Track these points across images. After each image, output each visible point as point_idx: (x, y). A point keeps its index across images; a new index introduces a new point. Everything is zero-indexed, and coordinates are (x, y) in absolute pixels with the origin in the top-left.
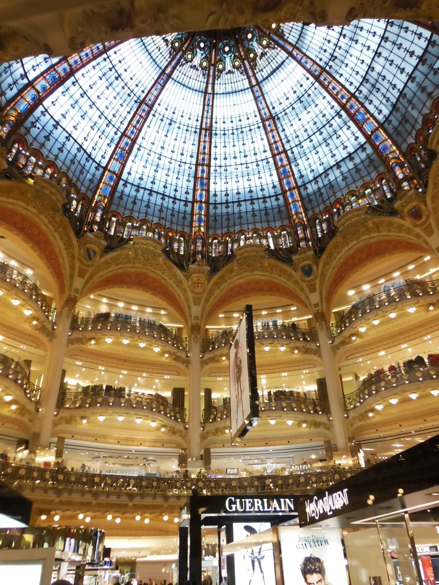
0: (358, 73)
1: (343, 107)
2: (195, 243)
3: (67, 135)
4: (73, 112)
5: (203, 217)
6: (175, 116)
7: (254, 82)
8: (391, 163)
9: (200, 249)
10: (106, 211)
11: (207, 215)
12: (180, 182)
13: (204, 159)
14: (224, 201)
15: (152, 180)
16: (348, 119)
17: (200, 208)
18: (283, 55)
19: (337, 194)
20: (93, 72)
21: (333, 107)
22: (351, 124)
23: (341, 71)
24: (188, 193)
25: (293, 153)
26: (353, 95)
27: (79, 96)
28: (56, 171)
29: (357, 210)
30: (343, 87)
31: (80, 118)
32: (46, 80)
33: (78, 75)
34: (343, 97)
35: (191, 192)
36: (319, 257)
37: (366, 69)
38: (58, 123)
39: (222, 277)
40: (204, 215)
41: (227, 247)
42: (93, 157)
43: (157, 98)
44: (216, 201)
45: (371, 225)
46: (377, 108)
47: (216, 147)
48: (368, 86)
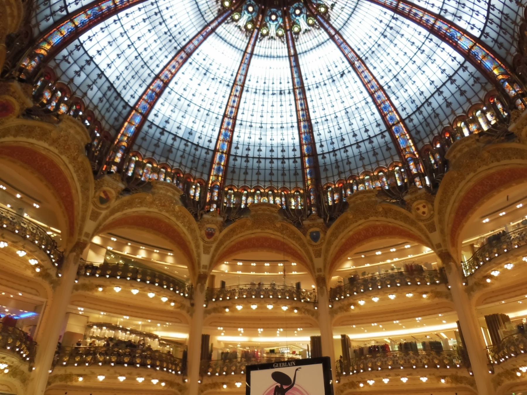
1: (371, 95)
2: (212, 192)
3: (100, 73)
4: (109, 49)
5: (222, 167)
8: (406, 157)
9: (216, 198)
10: (127, 151)
11: (226, 165)
12: (205, 130)
13: (231, 112)
14: (244, 155)
17: (221, 158)
18: (326, 36)
20: (138, 13)
27: (119, 34)
28: (83, 109)
29: (370, 191)
30: (374, 78)
31: (116, 56)
32: (87, 15)
33: (122, 14)
34: (373, 87)
36: (328, 226)
38: (91, 58)
39: (233, 231)
40: (224, 165)
41: (241, 200)
42: (122, 96)
43: (196, 48)
44: (236, 153)
45: (381, 209)
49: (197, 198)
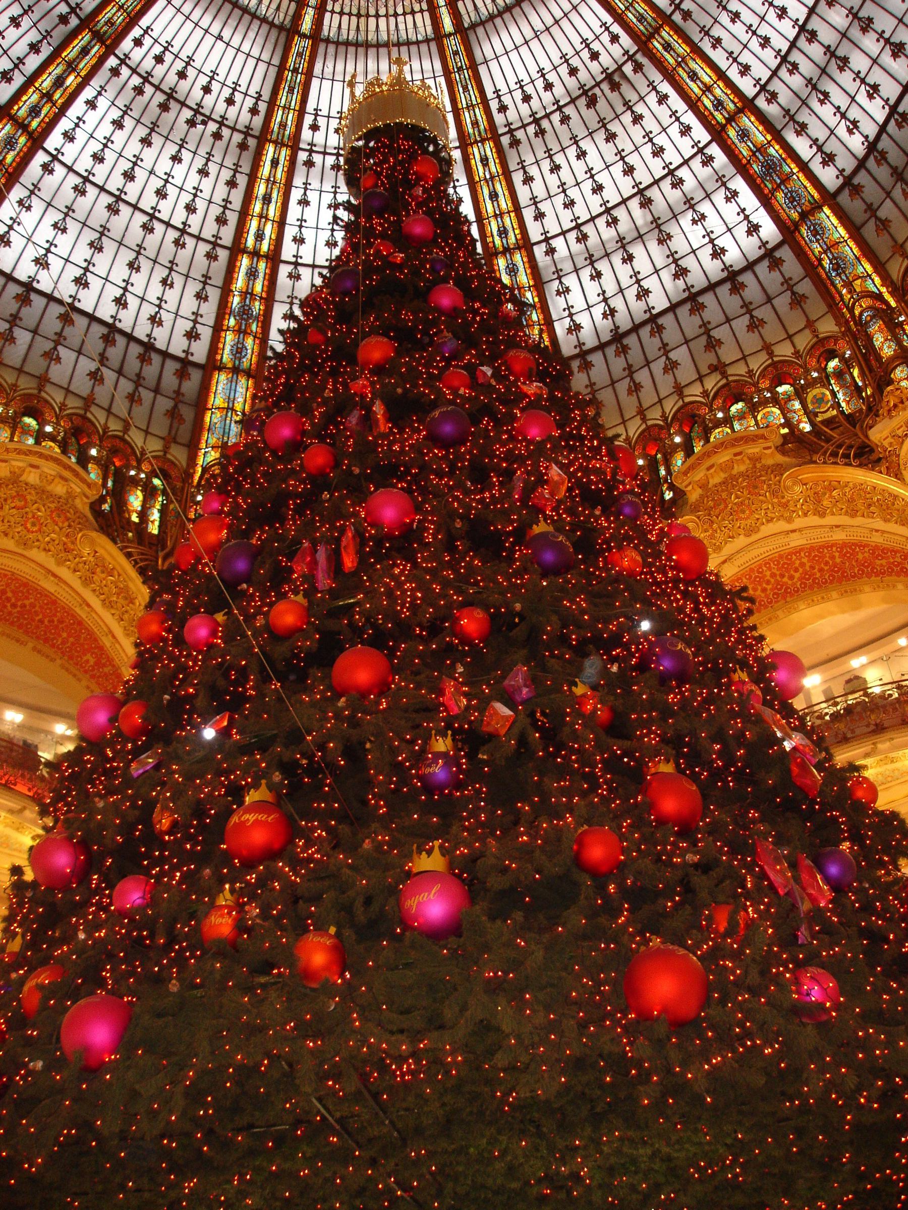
0: (765, 42)
1: (718, 134)
6: (184, 85)
7: (448, 25)
15: (78, 272)
16: (732, 170)
19: (687, 391)
21: (686, 130)
22: (739, 184)
23: (717, 32)
24: (197, 337)
25: (551, 251)
26: (748, 105)
30: (721, 75)
35: (206, 333)
37: (792, 33)
46: (820, 149)
47: (304, 202)
48: (796, 81)
49: (154, 529)
